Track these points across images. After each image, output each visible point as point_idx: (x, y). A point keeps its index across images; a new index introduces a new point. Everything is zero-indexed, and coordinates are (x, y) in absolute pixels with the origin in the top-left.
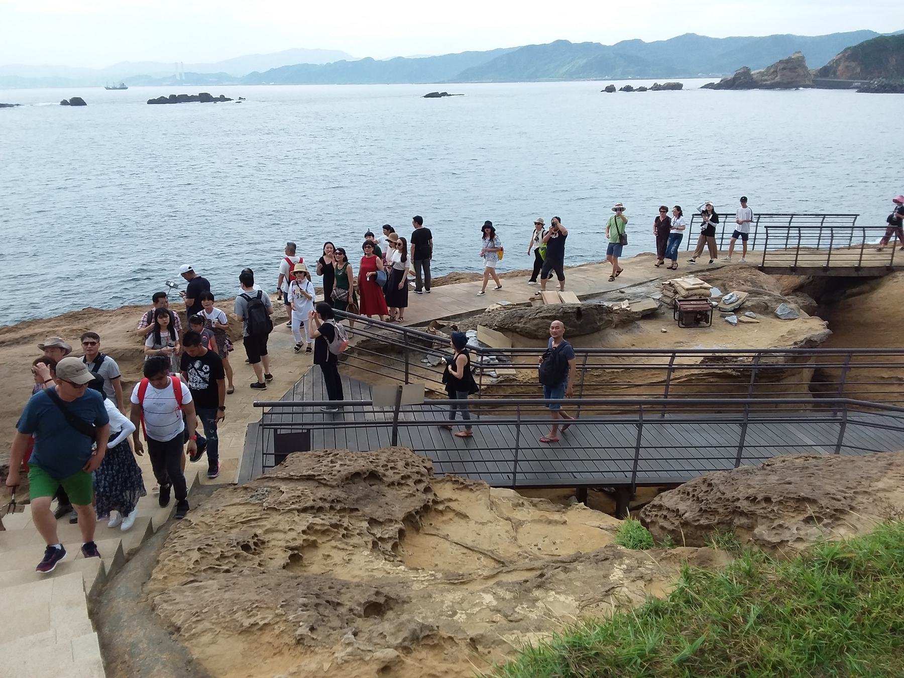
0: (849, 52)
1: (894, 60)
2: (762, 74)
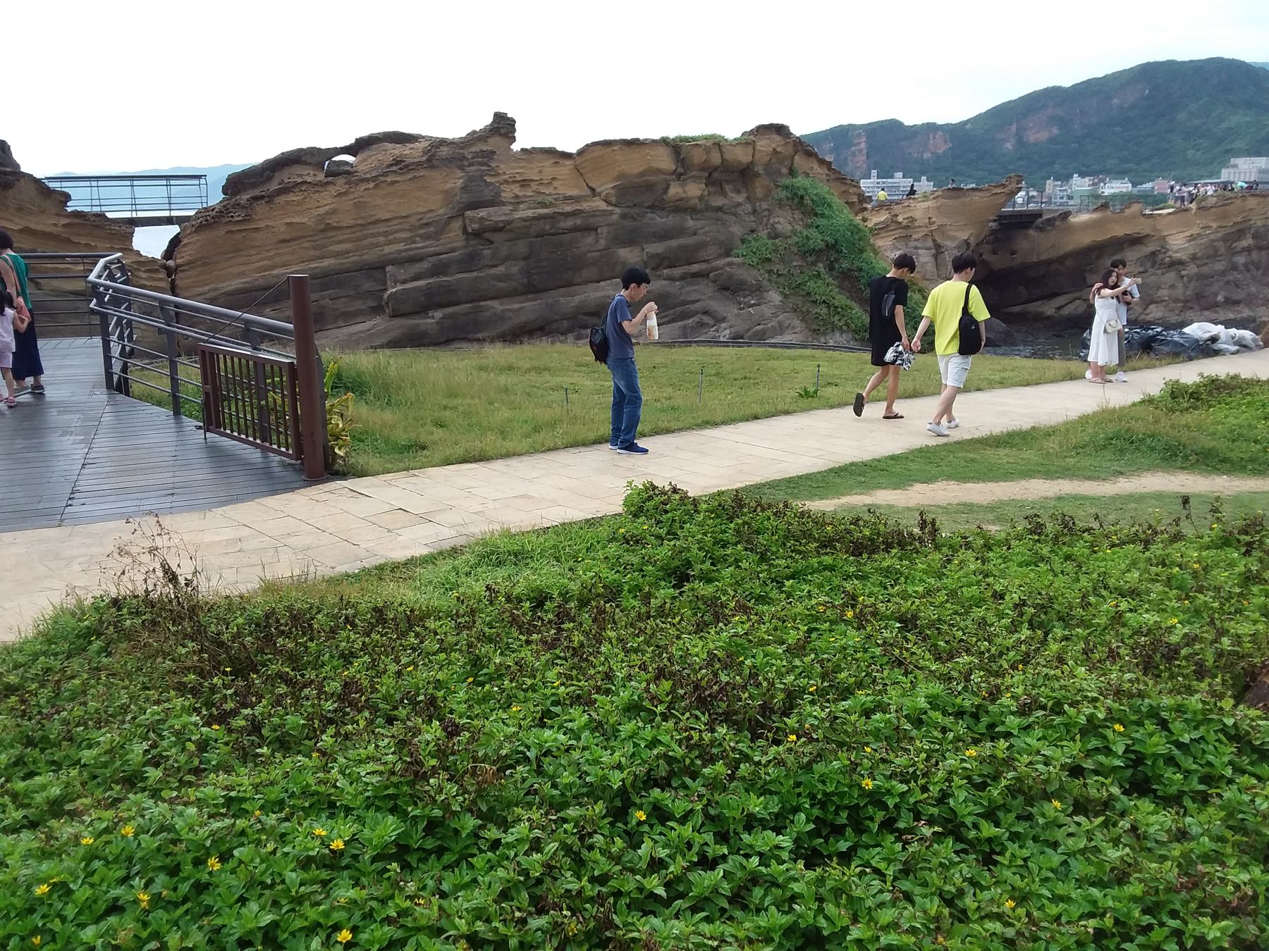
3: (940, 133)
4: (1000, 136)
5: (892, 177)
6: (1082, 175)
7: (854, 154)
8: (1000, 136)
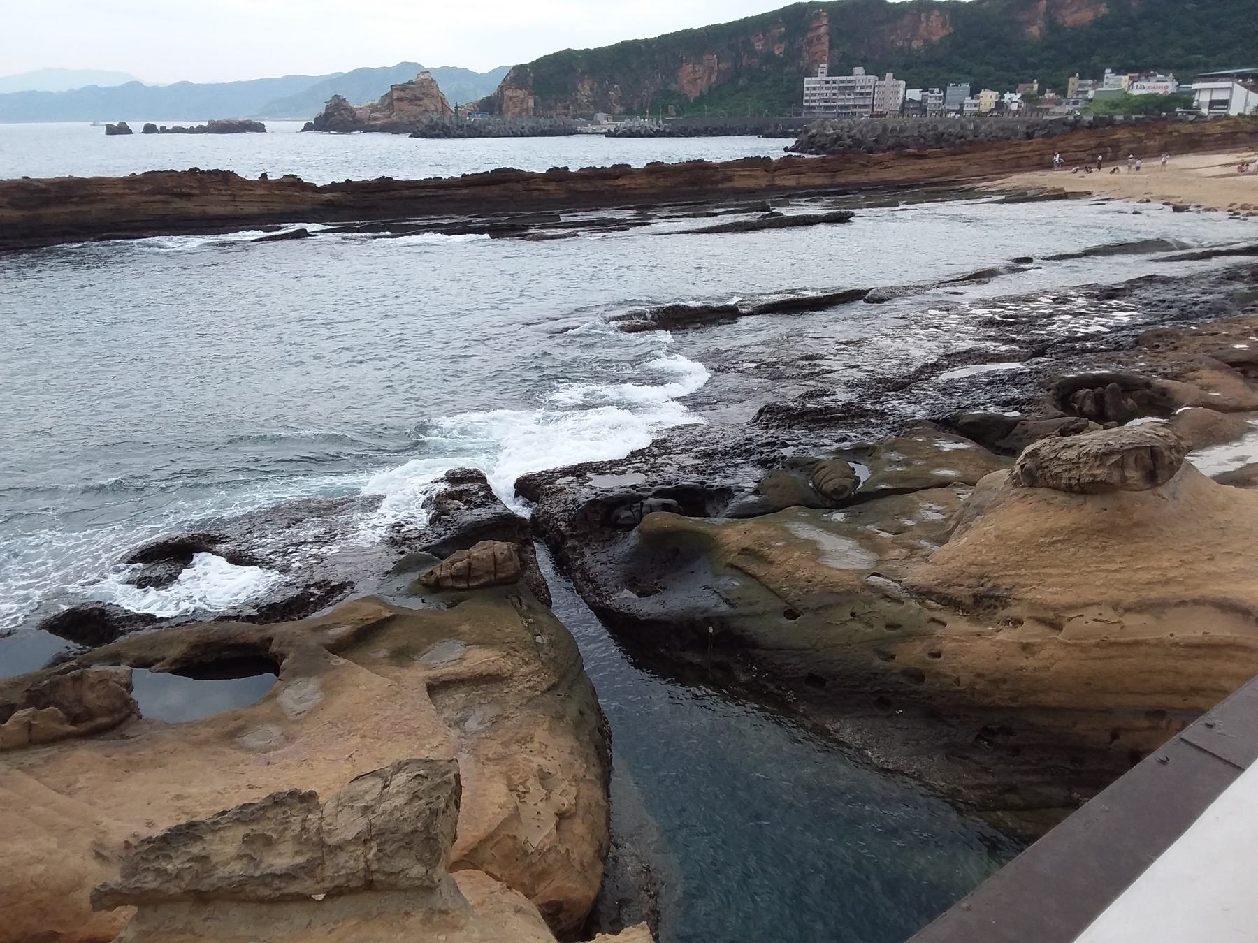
0: (512, 74)
1: (588, 88)
2: (373, 108)
3: (936, 13)
4: (1023, 17)
5: (851, 74)
6: (1118, 71)
7: (810, 43)
8: (1023, 17)
